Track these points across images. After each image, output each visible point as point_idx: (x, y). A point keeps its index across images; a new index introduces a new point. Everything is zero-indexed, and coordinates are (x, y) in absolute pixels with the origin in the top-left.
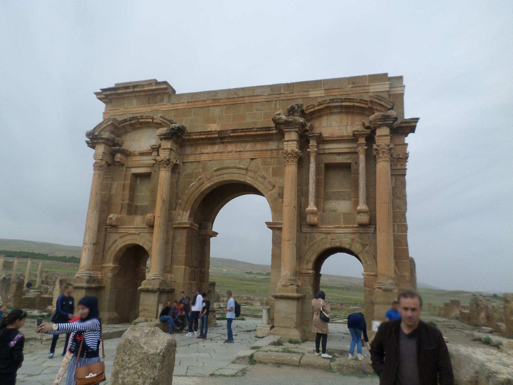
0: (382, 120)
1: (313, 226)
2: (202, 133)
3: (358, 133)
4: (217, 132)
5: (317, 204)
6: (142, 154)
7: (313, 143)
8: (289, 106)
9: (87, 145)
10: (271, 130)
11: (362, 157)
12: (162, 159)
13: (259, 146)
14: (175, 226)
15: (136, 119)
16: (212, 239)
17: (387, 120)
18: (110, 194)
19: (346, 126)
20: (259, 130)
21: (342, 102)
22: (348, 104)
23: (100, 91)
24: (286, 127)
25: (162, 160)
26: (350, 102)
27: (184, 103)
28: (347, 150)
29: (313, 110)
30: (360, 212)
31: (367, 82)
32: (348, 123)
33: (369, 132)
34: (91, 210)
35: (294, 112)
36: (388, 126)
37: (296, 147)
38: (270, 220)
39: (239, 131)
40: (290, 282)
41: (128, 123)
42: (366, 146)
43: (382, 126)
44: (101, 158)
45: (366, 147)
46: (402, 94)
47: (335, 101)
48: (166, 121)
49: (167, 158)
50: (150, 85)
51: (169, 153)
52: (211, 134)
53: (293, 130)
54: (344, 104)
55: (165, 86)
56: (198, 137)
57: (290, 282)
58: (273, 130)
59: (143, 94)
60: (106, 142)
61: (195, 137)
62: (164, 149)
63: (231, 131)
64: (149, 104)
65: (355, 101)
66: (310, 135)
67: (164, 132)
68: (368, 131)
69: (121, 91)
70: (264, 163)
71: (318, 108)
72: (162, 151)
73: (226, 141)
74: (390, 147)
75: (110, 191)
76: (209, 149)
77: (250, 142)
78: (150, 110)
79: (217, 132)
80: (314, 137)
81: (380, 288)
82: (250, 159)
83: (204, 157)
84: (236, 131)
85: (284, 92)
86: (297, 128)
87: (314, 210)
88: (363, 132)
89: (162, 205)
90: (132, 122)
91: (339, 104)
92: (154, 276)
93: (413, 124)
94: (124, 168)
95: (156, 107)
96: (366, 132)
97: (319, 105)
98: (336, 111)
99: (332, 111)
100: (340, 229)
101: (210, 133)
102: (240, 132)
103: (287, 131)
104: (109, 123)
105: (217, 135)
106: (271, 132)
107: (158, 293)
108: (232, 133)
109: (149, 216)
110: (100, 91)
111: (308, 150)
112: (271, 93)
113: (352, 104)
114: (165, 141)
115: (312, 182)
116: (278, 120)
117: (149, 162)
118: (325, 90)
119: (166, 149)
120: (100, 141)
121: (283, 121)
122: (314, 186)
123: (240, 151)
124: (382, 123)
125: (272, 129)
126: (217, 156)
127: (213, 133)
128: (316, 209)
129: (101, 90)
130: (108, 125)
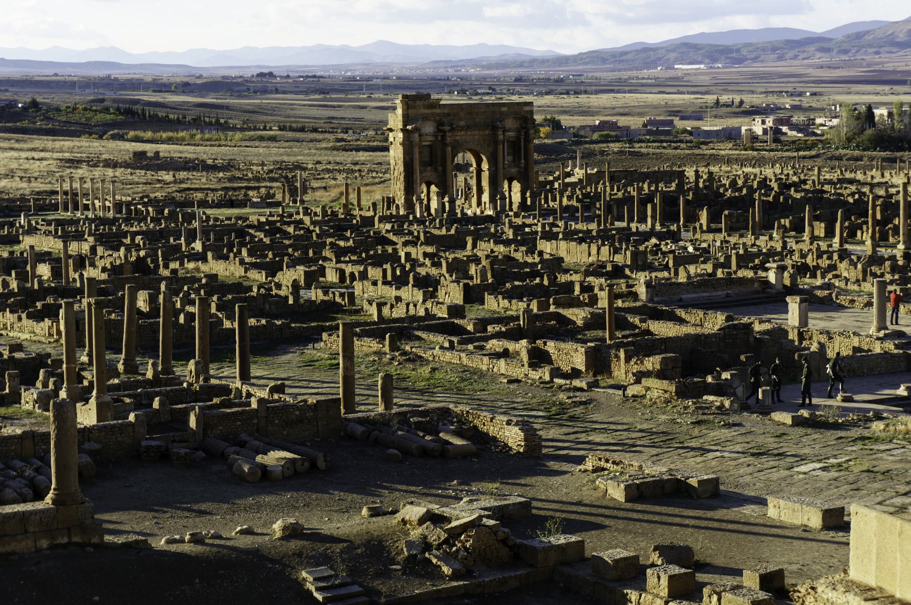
11: (522, 140)
70: (484, 140)
83: (458, 138)
95: (434, 111)
126: (464, 137)
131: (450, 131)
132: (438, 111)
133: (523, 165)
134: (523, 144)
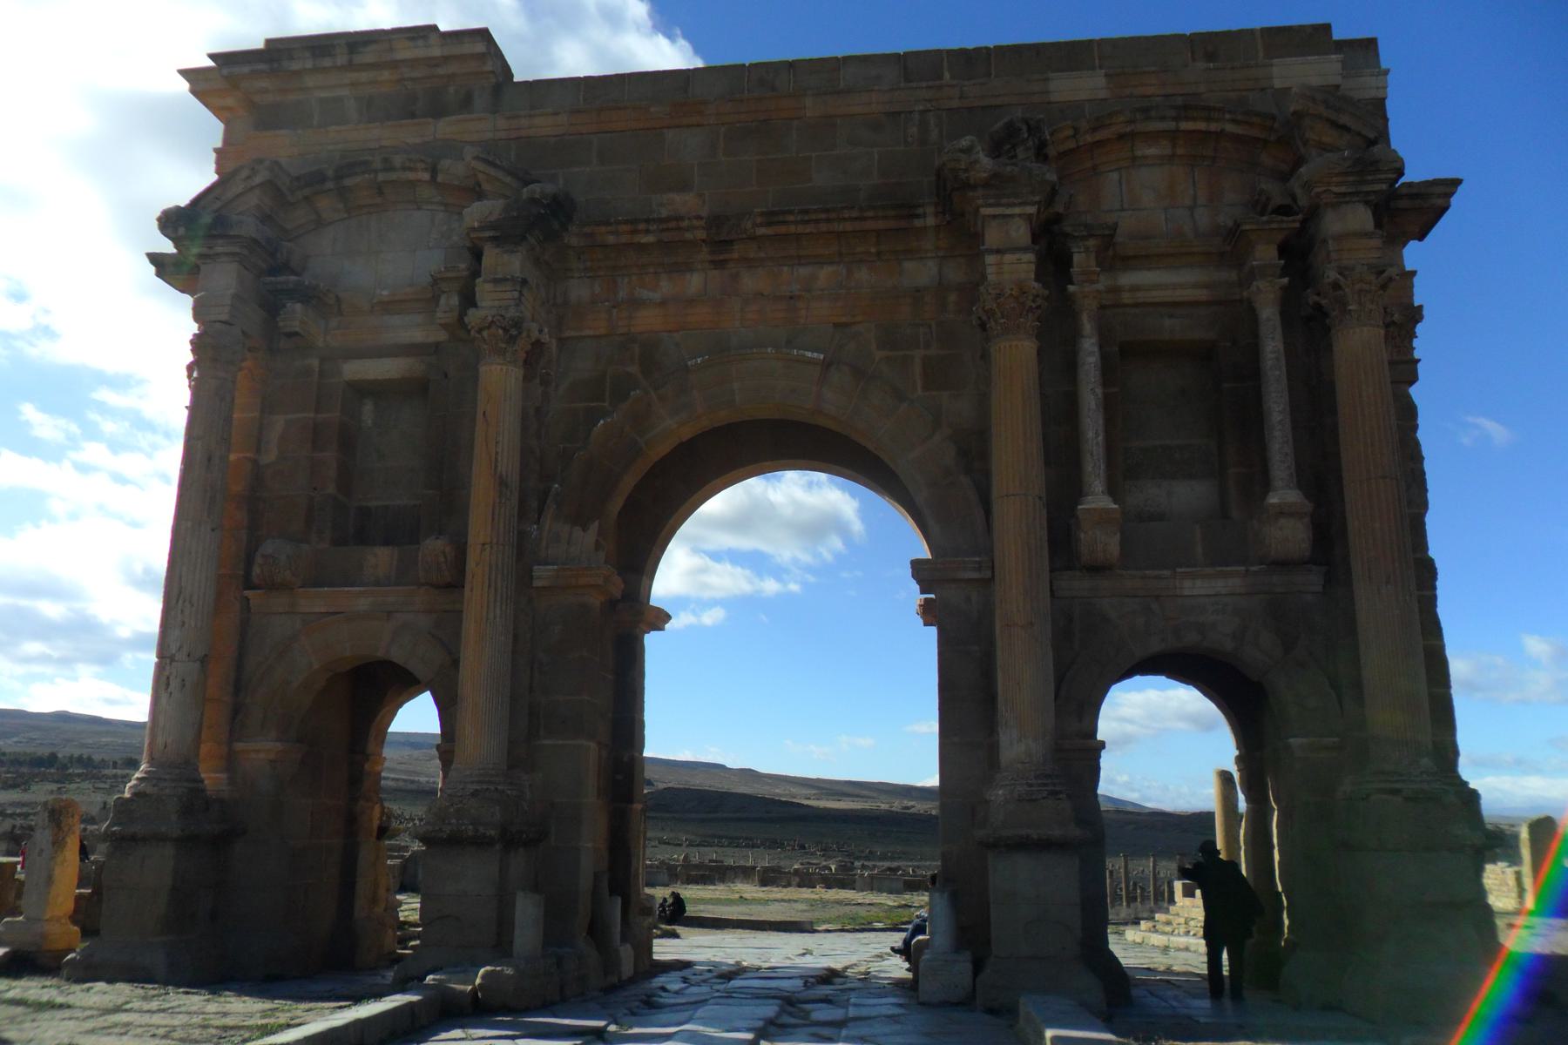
0: (1351, 179)
1: (1097, 569)
2: (642, 226)
3: (1254, 227)
4: (702, 223)
5: (1112, 490)
6: (389, 307)
7: (1081, 259)
8: (1000, 124)
9: (152, 269)
10: (918, 216)
11: (1269, 313)
12: (490, 319)
13: (863, 275)
14: (537, 583)
15: (363, 173)
16: (651, 640)
17: (1370, 178)
18: (255, 462)
19: (1192, 209)
20: (870, 214)
21: (1176, 119)
22: (1202, 126)
23: (210, 63)
24: (992, 201)
25: (492, 321)
26: (1208, 119)
27: (556, 114)
28: (1202, 294)
29: (1071, 145)
30: (1283, 512)
31: (1261, 54)
32: (1195, 198)
33: (1297, 225)
34: (189, 524)
35: (1014, 147)
36: (1367, 203)
37: (1033, 276)
38: (925, 553)
39: (791, 218)
40: (1045, 785)
41: (330, 185)
42: (1281, 276)
43: (1347, 203)
44: (224, 317)
45: (1285, 280)
46: (1380, 104)
47: (1153, 113)
48: (500, 175)
49: (512, 313)
50: (420, 43)
51: (516, 294)
52: (679, 229)
53: (1017, 210)
54: (1185, 126)
55: (480, 48)
56: (624, 239)
57: (1045, 785)
58: (924, 215)
59: (386, 75)
60: (245, 252)
61: (611, 239)
62: (496, 281)
63: (759, 220)
64: (413, 115)
65: (1227, 116)
66: (1076, 234)
67: (493, 218)
68: (1293, 222)
69: (295, 66)
71: (1089, 138)
72: (488, 287)
73: (736, 255)
74: (1385, 275)
75: (258, 450)
76: (666, 287)
77: (831, 263)
78: (418, 141)
79: (702, 223)
80: (1091, 242)
81: (1396, 792)
82: (831, 325)
83: (647, 320)
84: (781, 218)
85: (955, 82)
86: (1032, 204)
87: (1107, 511)
88: (1274, 226)
89: (498, 501)
90: (348, 182)
91: (1171, 125)
92: (479, 782)
93: (1440, 202)
94: (315, 363)
96: (1284, 226)
97: (1094, 130)
98: (1152, 151)
99: (1139, 153)
100: (1199, 583)
101: (673, 224)
102: (796, 223)
103: (994, 217)
104: (258, 180)
105: (701, 234)
106: (918, 223)
107: (498, 847)
108: (761, 225)
109: (434, 547)
110: (210, 63)
111: (1071, 288)
112: (902, 85)
113: (1214, 127)
114: (497, 251)
115: (1093, 405)
116: (966, 170)
117: (418, 336)
118: (1106, 75)
119: (504, 280)
120: (219, 249)
121: (985, 175)
122: (1101, 422)
123: (791, 298)
124: (1350, 190)
125: (920, 211)
127: (685, 223)
128: (1106, 503)
129: (212, 56)
130: (252, 188)
131: (505, 234)
132: (476, 127)
133: (1292, 536)
134: (1272, 347)
